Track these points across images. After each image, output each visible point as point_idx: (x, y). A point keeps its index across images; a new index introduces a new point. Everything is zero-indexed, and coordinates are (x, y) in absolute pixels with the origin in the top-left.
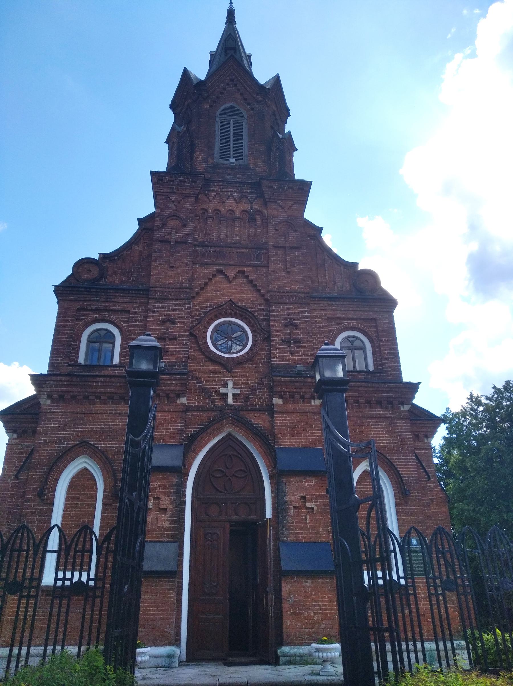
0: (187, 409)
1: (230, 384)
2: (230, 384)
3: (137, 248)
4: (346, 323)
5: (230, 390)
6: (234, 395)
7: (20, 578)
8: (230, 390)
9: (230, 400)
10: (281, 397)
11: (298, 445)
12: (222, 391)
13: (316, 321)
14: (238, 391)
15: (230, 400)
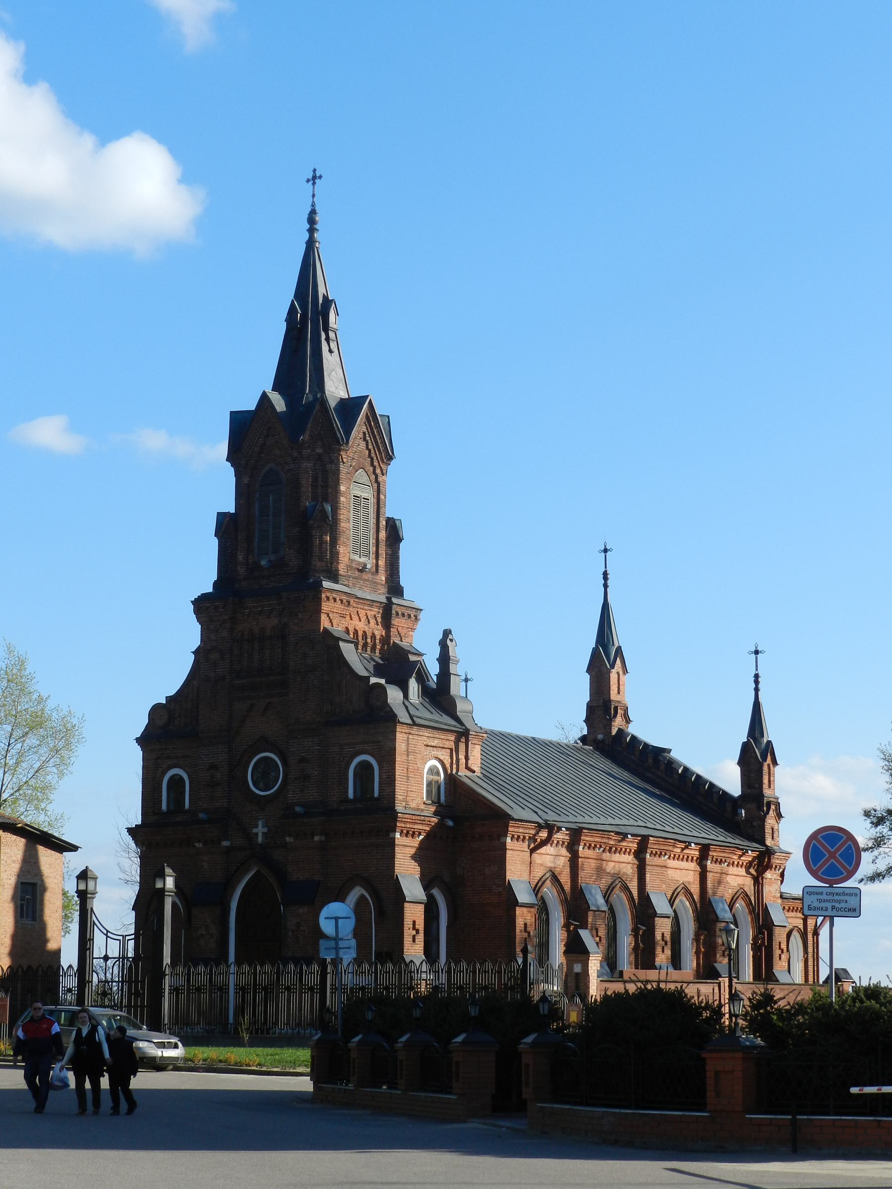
0: (228, 850)
1: (260, 823)
2: (260, 823)
3: (195, 683)
4: (359, 747)
5: (260, 830)
6: (263, 833)
7: (71, 987)
8: (260, 830)
9: (260, 839)
10: (290, 836)
11: (303, 878)
12: (255, 831)
13: (331, 749)
14: (266, 830)
15: (260, 839)
